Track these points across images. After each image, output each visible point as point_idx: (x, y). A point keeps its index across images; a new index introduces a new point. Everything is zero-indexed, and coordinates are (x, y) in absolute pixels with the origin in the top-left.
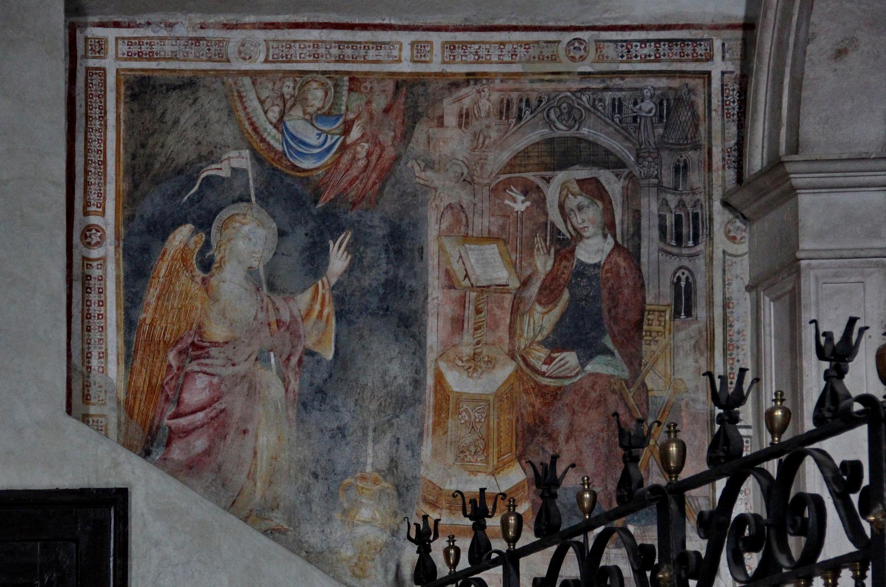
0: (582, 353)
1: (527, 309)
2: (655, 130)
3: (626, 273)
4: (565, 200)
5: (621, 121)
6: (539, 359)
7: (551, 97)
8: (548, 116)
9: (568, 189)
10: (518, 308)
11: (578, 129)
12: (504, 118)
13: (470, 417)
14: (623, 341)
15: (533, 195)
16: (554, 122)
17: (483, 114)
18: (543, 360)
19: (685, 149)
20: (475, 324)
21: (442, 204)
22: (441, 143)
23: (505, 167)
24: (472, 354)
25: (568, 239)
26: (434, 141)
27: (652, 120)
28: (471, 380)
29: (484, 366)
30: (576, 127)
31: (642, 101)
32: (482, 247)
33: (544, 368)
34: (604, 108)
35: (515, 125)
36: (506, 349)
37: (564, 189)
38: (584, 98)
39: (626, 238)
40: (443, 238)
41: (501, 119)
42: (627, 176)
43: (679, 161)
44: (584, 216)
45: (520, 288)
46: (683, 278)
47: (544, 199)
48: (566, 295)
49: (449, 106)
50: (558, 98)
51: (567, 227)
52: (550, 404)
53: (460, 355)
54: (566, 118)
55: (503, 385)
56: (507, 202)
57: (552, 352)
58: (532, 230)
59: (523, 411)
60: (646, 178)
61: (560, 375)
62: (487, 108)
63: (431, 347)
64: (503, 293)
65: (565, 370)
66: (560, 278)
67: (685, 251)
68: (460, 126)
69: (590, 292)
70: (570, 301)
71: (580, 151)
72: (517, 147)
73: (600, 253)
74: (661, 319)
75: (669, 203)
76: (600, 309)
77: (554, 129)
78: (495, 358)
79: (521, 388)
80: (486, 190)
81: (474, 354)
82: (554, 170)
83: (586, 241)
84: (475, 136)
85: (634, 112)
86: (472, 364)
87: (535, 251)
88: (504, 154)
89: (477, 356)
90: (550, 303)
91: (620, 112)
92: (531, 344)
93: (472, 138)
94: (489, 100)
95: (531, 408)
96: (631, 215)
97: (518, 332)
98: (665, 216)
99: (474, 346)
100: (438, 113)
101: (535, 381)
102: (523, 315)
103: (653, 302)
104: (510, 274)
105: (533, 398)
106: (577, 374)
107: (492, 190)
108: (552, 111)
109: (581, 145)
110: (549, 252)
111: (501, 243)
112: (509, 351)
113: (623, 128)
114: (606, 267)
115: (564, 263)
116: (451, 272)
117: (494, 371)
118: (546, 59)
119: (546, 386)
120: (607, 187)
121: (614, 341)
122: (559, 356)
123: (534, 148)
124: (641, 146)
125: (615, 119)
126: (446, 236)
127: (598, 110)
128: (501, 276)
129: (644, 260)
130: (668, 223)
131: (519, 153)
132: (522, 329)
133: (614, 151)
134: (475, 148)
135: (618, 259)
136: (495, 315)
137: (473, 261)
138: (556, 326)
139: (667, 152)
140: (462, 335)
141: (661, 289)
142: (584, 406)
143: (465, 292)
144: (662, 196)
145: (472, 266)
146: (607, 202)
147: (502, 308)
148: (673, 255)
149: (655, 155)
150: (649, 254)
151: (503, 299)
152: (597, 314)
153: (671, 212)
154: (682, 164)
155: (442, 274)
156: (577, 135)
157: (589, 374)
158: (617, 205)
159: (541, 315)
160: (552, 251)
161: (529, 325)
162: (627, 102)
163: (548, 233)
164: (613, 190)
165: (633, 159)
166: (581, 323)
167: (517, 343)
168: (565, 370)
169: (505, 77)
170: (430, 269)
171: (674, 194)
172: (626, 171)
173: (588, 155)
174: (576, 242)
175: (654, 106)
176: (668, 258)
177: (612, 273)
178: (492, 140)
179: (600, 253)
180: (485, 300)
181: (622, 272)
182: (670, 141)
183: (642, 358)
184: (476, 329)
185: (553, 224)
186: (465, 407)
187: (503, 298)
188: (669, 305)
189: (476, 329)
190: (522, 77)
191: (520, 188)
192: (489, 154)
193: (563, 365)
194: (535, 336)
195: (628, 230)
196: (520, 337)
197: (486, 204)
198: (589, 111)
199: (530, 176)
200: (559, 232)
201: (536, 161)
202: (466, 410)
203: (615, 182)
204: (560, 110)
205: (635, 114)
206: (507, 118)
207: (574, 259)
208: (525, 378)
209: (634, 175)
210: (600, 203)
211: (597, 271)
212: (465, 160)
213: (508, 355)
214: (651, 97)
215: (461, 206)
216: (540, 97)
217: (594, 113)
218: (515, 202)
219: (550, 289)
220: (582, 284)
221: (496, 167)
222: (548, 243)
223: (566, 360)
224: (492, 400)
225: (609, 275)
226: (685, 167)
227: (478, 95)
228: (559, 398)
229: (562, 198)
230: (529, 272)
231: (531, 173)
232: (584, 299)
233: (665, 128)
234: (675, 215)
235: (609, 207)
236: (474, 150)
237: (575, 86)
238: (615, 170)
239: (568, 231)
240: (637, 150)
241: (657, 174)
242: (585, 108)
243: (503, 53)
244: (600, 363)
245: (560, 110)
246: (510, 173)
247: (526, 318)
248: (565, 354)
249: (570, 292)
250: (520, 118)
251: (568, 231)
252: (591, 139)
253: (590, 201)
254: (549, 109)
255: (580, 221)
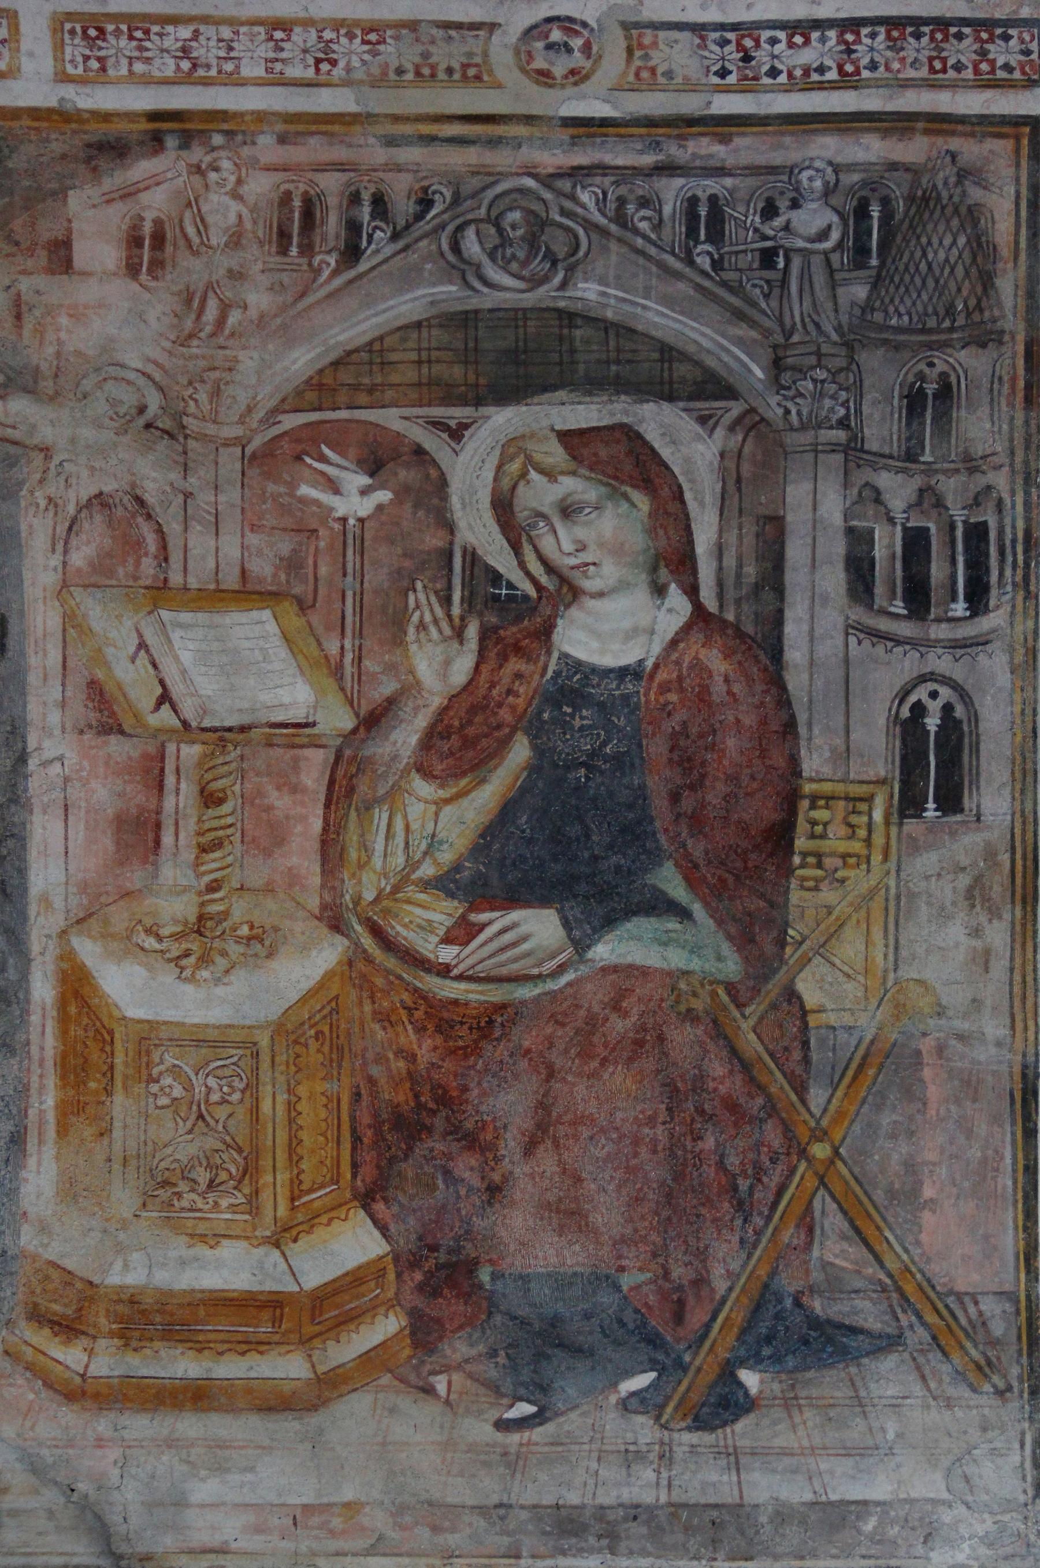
0: (577, 911)
1: (381, 792)
2: (840, 291)
3: (729, 693)
4: (514, 487)
5: (717, 265)
6: (428, 927)
7: (466, 189)
8: (456, 247)
9: (529, 458)
10: (351, 790)
11: (563, 285)
12: (294, 251)
13: (189, 1087)
14: (722, 880)
15: (403, 474)
16: (478, 266)
17: (216, 238)
18: (441, 932)
19: (946, 344)
20: (200, 834)
21: (72, 495)
22: (64, 321)
23: (299, 393)
24: (192, 919)
25: (526, 598)
26: (37, 313)
27: (828, 262)
28: (189, 988)
29: (234, 949)
30: (557, 280)
31: (795, 205)
32: (217, 619)
33: (447, 954)
34: (658, 225)
35: (336, 273)
36: (314, 903)
37: (512, 459)
38: (585, 197)
39: (730, 594)
40: (76, 591)
41: (284, 251)
42: (738, 421)
43: (921, 377)
44: (581, 533)
45: (355, 731)
46: (934, 707)
47: (443, 483)
48: (520, 752)
49: (91, 213)
50: (490, 194)
51: (522, 565)
52: (473, 1050)
53: (148, 922)
54: (521, 254)
55: (304, 1000)
56: (305, 490)
57: (473, 908)
58: (399, 571)
59: (375, 1071)
60: (803, 427)
61: (504, 971)
62: (232, 219)
63: (45, 900)
64: (293, 746)
65: (516, 960)
66: (500, 705)
67: (940, 632)
68: (132, 270)
69: (604, 744)
70: (534, 769)
71: (573, 351)
72: (341, 338)
73: (643, 639)
74: (854, 819)
75: (886, 497)
76: (641, 794)
77: (477, 284)
78: (276, 929)
79: (368, 1008)
80: (230, 462)
81: (201, 918)
82: (478, 402)
83: (591, 603)
84: (189, 301)
85: (765, 238)
86: (194, 945)
87: (411, 630)
88: (295, 354)
89: (209, 924)
90: (464, 774)
91: (716, 235)
92: (396, 889)
93: (178, 309)
94: (236, 196)
95: (402, 1064)
96: (750, 529)
97: (353, 854)
98: (871, 531)
99: (200, 894)
100: (48, 229)
101: (416, 990)
102: (367, 809)
103: (827, 771)
104: (320, 692)
105: (408, 1037)
106: (562, 969)
107: (254, 456)
108: (470, 233)
109: (578, 333)
110: (459, 635)
111: (289, 608)
112: (324, 907)
113: (724, 284)
114: (662, 676)
115: (515, 664)
116: (110, 687)
117: (274, 964)
118: (442, 75)
119: (455, 1002)
120: (665, 453)
121: (692, 882)
122: (496, 920)
123: (404, 340)
124: (788, 334)
125: (699, 260)
126: (85, 586)
127: (636, 232)
128: (286, 700)
129: (795, 654)
130: (879, 553)
131: (349, 353)
132: (365, 847)
133: (691, 349)
134: (191, 336)
135: (703, 652)
136: (270, 808)
137: (186, 657)
138: (482, 836)
139: (880, 352)
140: (155, 864)
141: (853, 736)
142: (586, 1054)
143: (163, 746)
144: (866, 475)
145: (184, 672)
146: (665, 492)
147: (295, 789)
148: (898, 642)
149: (840, 362)
150: (812, 640)
151: (296, 767)
152: (630, 807)
153: (891, 521)
154: (931, 388)
155: (77, 695)
156: (562, 304)
157: (604, 970)
158: (702, 504)
159: (433, 808)
160: (472, 631)
161: (389, 835)
162: (742, 209)
163: (457, 581)
164: (687, 460)
165: (759, 373)
166: (574, 830)
167: (349, 888)
168: (516, 960)
169: (292, 128)
170: (33, 679)
171: (903, 471)
172: (736, 408)
173: (599, 362)
174: (555, 606)
175: (835, 219)
176: (880, 649)
177: (682, 690)
178: (253, 313)
179: (643, 639)
180: (234, 765)
181: (718, 689)
182: (894, 322)
183: (787, 924)
184: (203, 849)
185: (472, 558)
186: (169, 1060)
187: (296, 760)
188: (882, 782)
189: (203, 849)
190: (357, 128)
191: (352, 452)
192: (242, 355)
193: (514, 945)
194: (413, 865)
195: (739, 575)
196: (361, 866)
197: (231, 495)
198: (604, 233)
199: (391, 419)
200: (496, 578)
201: (411, 375)
202: (175, 1071)
203: (699, 438)
204: (500, 231)
205: (769, 244)
206: (307, 249)
207: (549, 653)
208: (379, 981)
209: (763, 419)
210: (636, 496)
211: (629, 687)
212: (150, 369)
213: (319, 919)
214: (828, 192)
215: (140, 501)
216: (425, 189)
217: (620, 240)
218: (337, 491)
219: (465, 739)
220: (577, 723)
221: (268, 389)
222: (456, 611)
223: (523, 929)
224: (264, 1042)
225: (673, 697)
226: (946, 392)
227: (196, 179)
228: (497, 1033)
229: (506, 483)
230: (388, 687)
231: (394, 411)
232: (583, 764)
233: (875, 286)
234: (905, 529)
235: (673, 507)
236: (186, 340)
237: (551, 159)
238: (692, 405)
239: (528, 574)
240: (775, 347)
241: (847, 416)
242: (589, 225)
243: (284, 55)
244: (639, 939)
245: (500, 231)
246: (320, 409)
247: (380, 816)
248: (515, 915)
249: (534, 747)
250: (352, 253)
251: (528, 574)
252: (609, 314)
253: (603, 489)
254: (460, 228)
255: (568, 546)
